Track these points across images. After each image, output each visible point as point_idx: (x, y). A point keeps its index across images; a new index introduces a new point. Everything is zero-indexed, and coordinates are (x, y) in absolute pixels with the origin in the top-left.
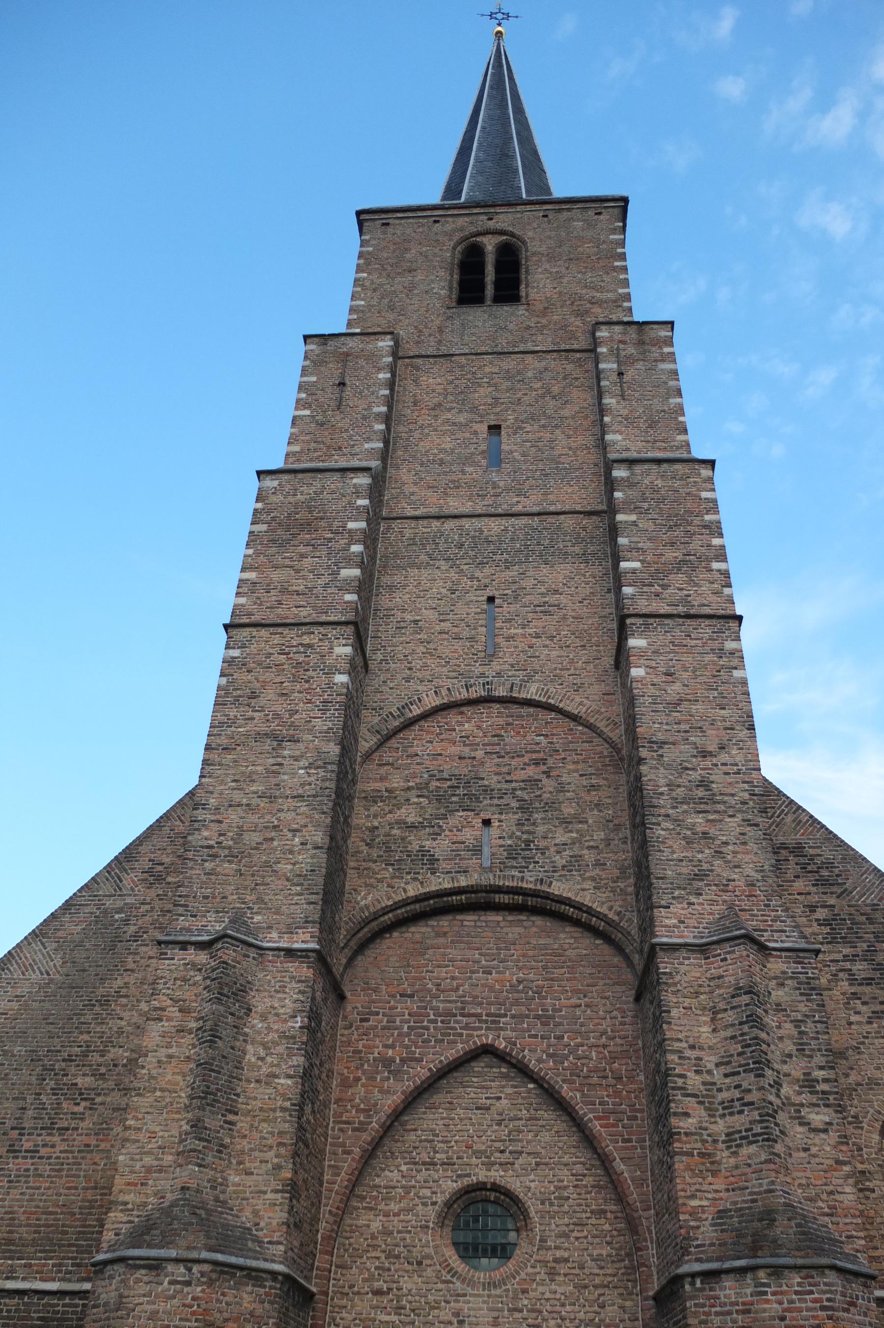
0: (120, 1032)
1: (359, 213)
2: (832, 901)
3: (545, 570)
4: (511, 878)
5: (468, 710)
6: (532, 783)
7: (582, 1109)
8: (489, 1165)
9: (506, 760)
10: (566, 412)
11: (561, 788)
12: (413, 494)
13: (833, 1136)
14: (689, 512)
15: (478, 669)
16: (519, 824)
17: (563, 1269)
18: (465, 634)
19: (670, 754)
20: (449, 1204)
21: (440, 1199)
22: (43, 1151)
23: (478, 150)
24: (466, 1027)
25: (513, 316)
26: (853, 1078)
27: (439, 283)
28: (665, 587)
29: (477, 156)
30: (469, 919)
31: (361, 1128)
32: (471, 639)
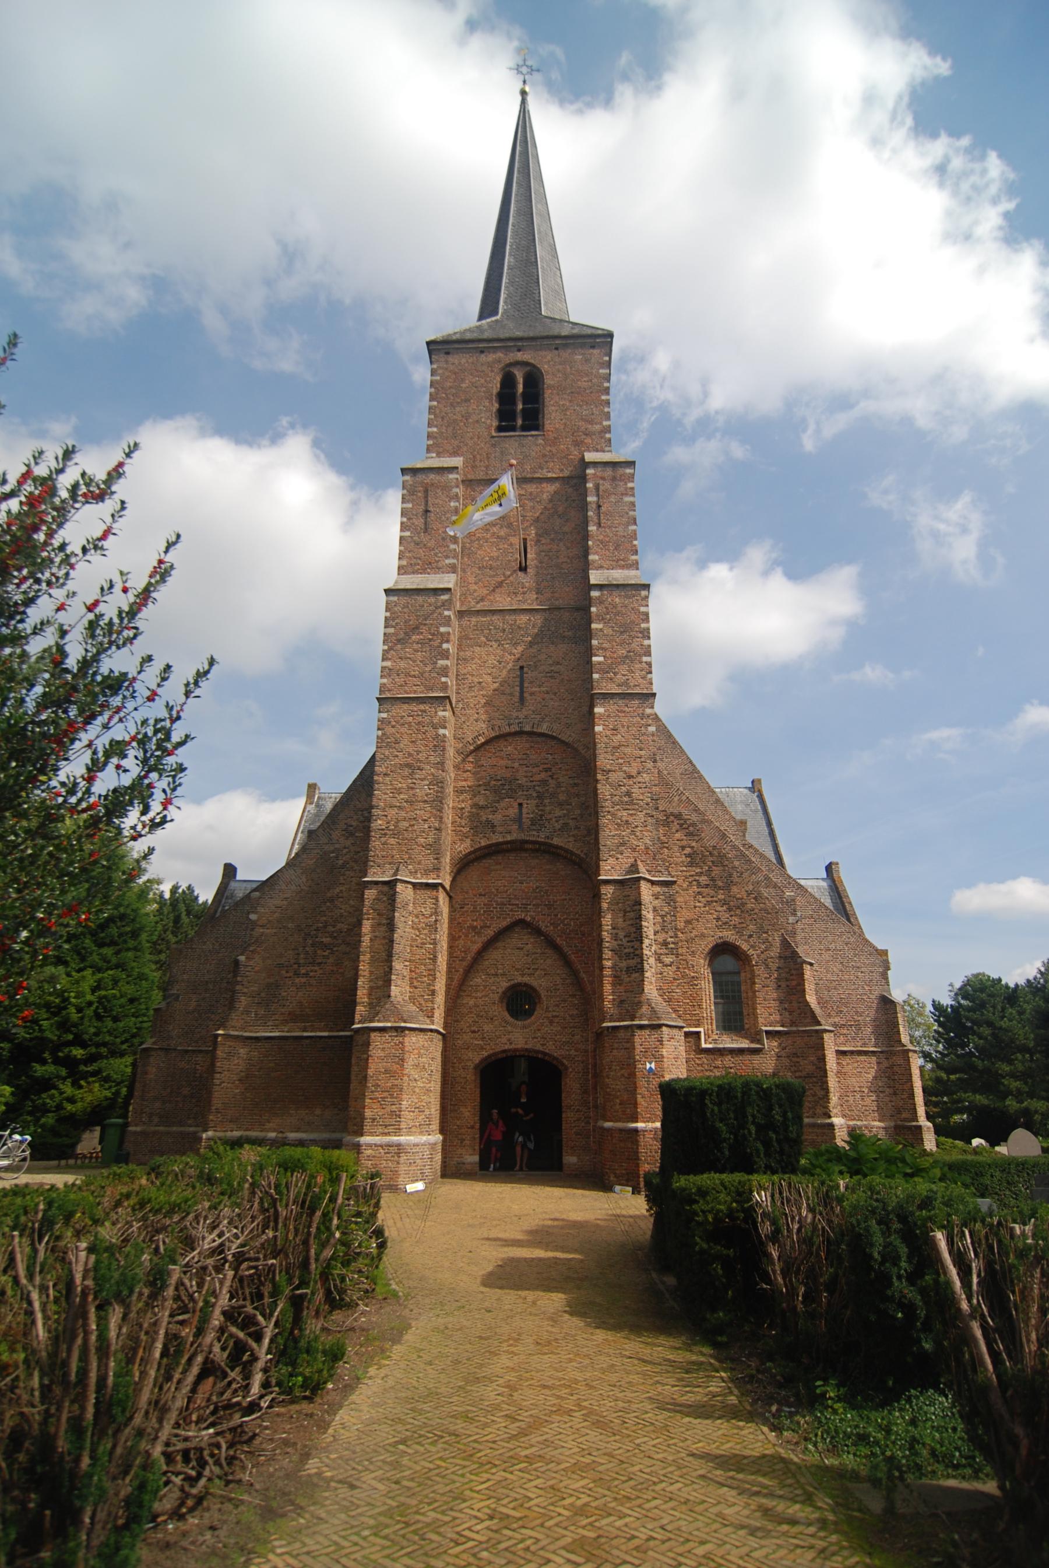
0: (341, 916)
1: (428, 343)
2: (694, 844)
3: (552, 648)
4: (533, 836)
5: (510, 739)
6: (544, 782)
7: (566, 949)
8: (523, 975)
9: (530, 769)
10: (566, 529)
11: (559, 785)
12: (475, 591)
13: (674, 968)
14: (632, 622)
15: (515, 714)
16: (537, 806)
17: (556, 1020)
18: (508, 691)
19: (613, 777)
20: (504, 993)
21: (500, 990)
22: (311, 974)
23: (510, 255)
24: (511, 910)
25: (533, 443)
26: (695, 932)
27: (485, 413)
28: (615, 674)
29: (509, 262)
30: (512, 856)
31: (463, 959)
32: (511, 694)
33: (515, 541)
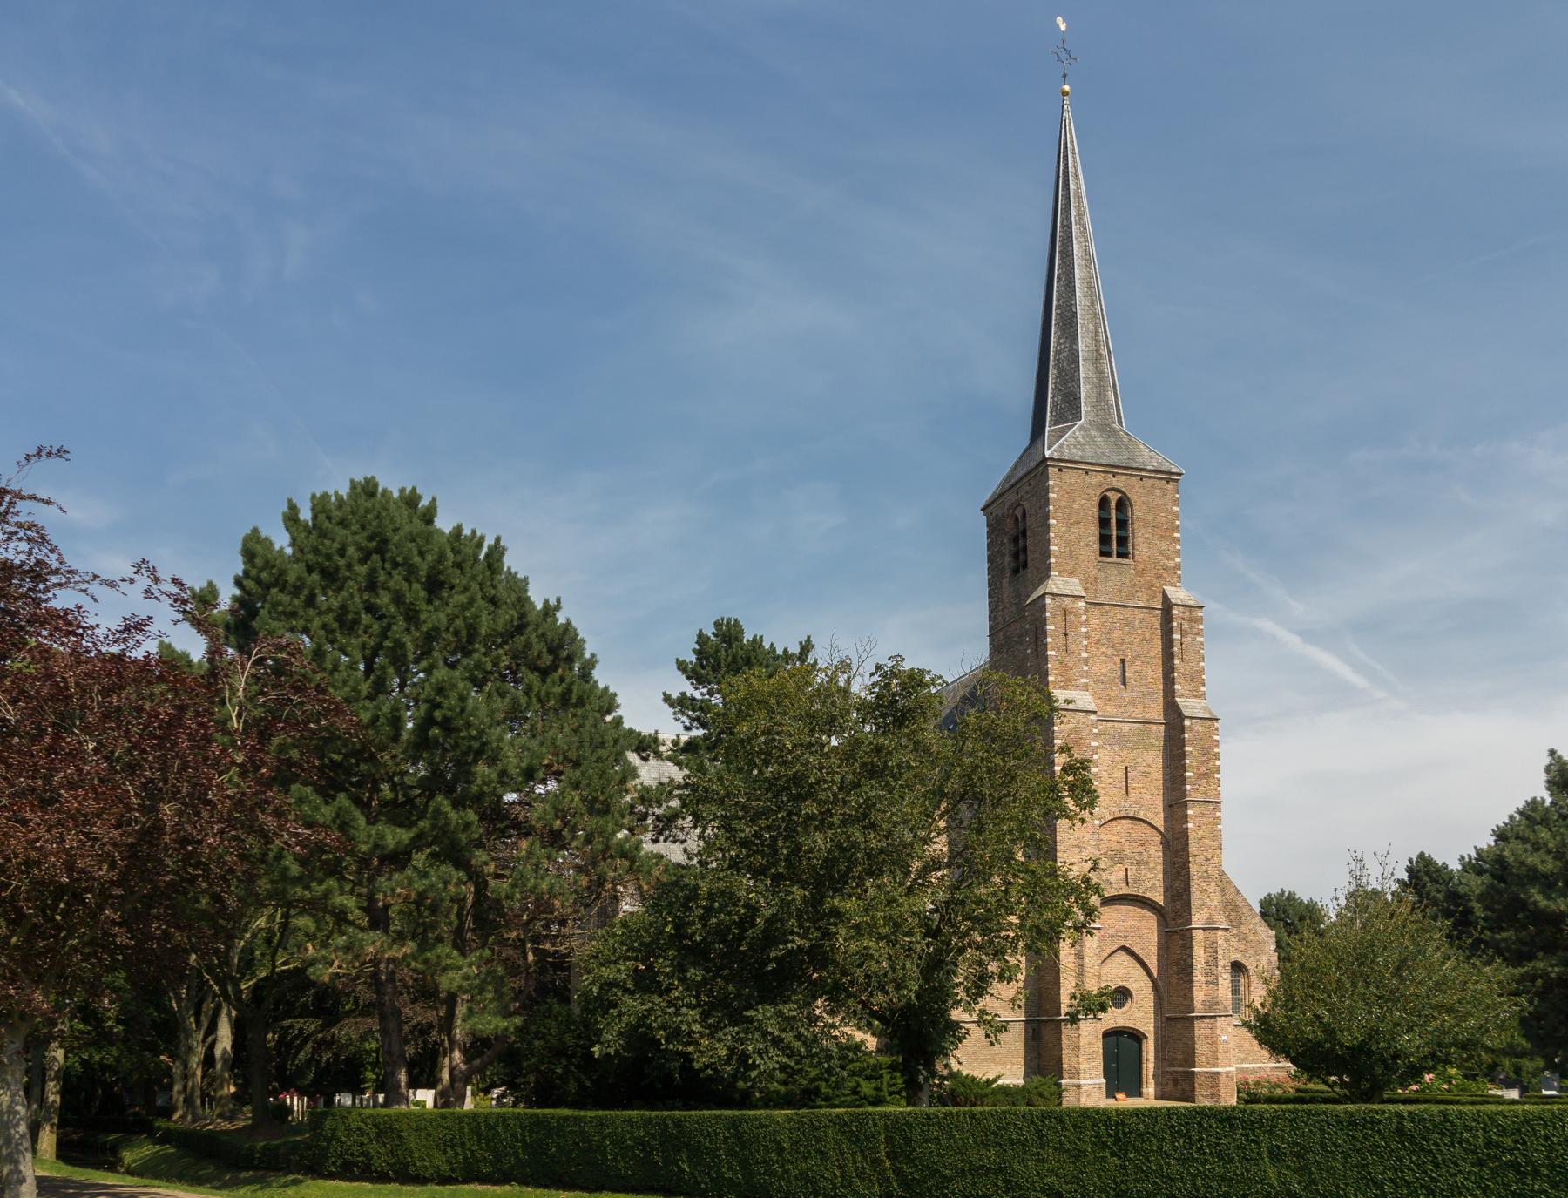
6: (1140, 854)
19: (1200, 859)
33: (1118, 660)
